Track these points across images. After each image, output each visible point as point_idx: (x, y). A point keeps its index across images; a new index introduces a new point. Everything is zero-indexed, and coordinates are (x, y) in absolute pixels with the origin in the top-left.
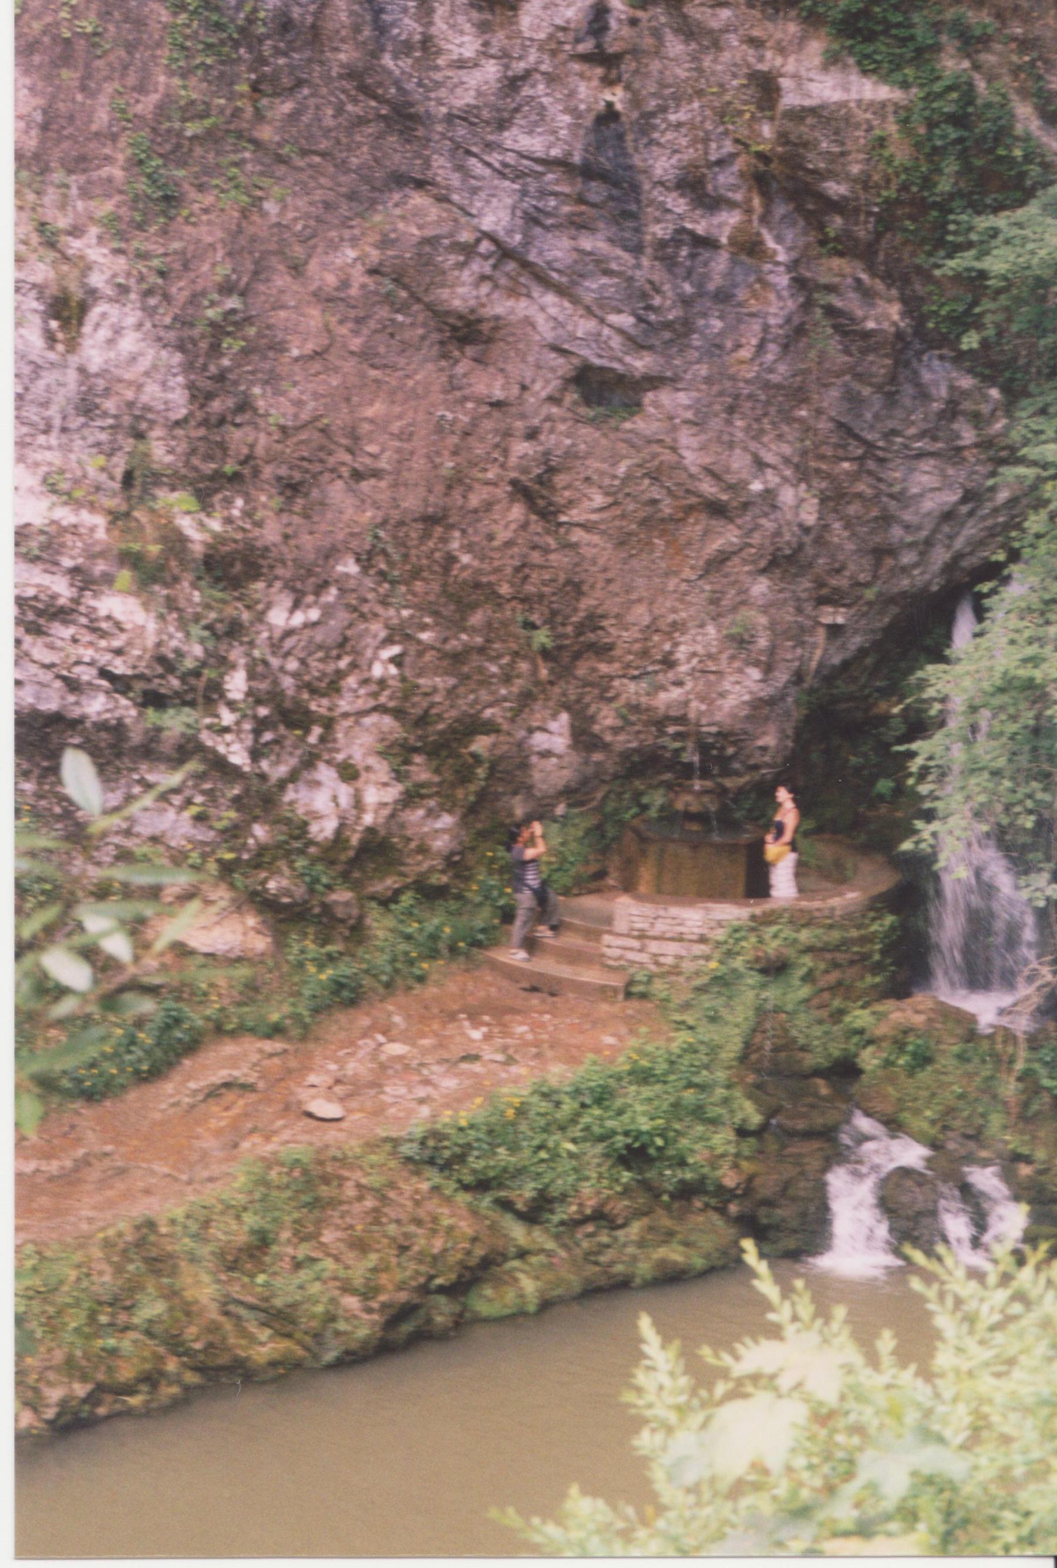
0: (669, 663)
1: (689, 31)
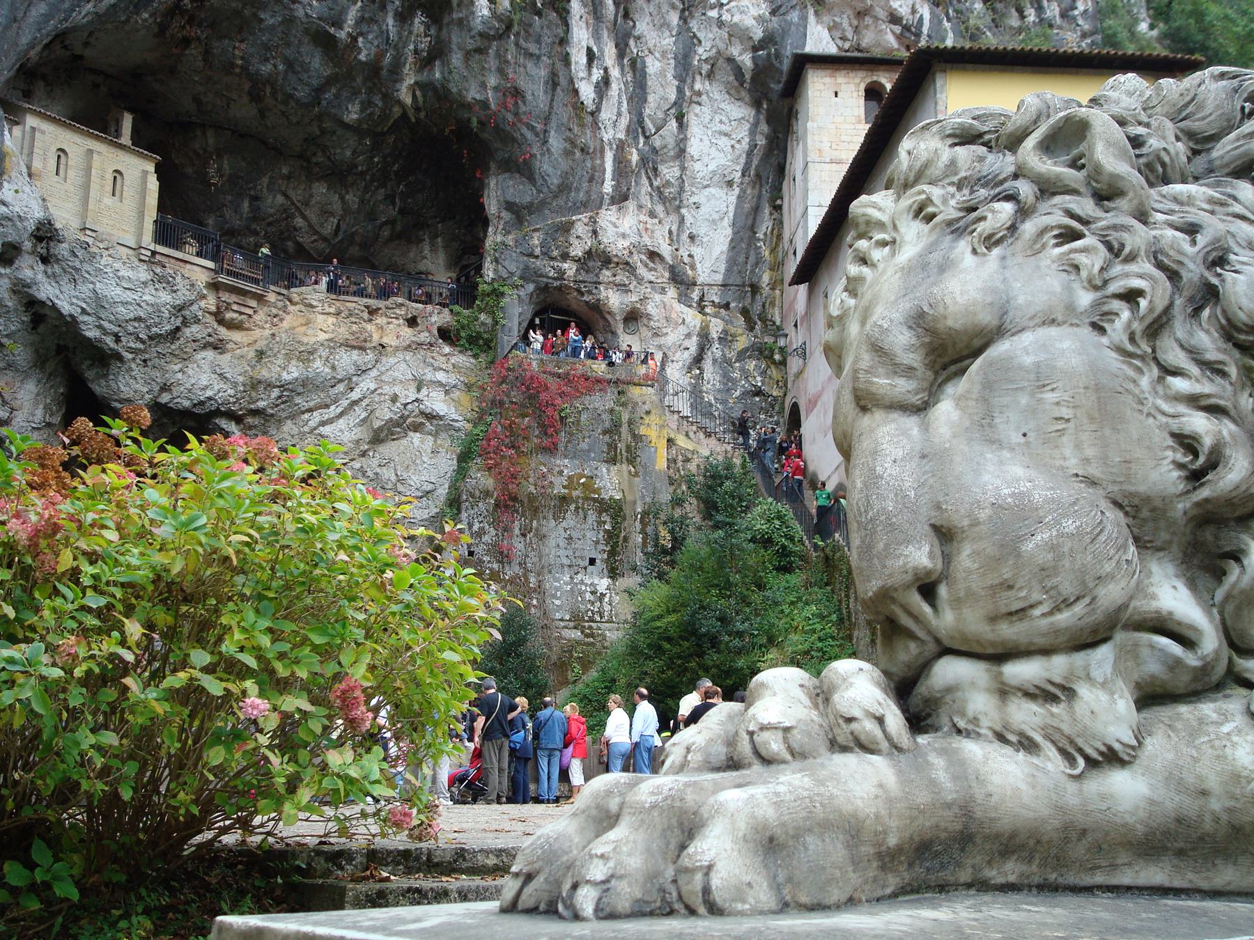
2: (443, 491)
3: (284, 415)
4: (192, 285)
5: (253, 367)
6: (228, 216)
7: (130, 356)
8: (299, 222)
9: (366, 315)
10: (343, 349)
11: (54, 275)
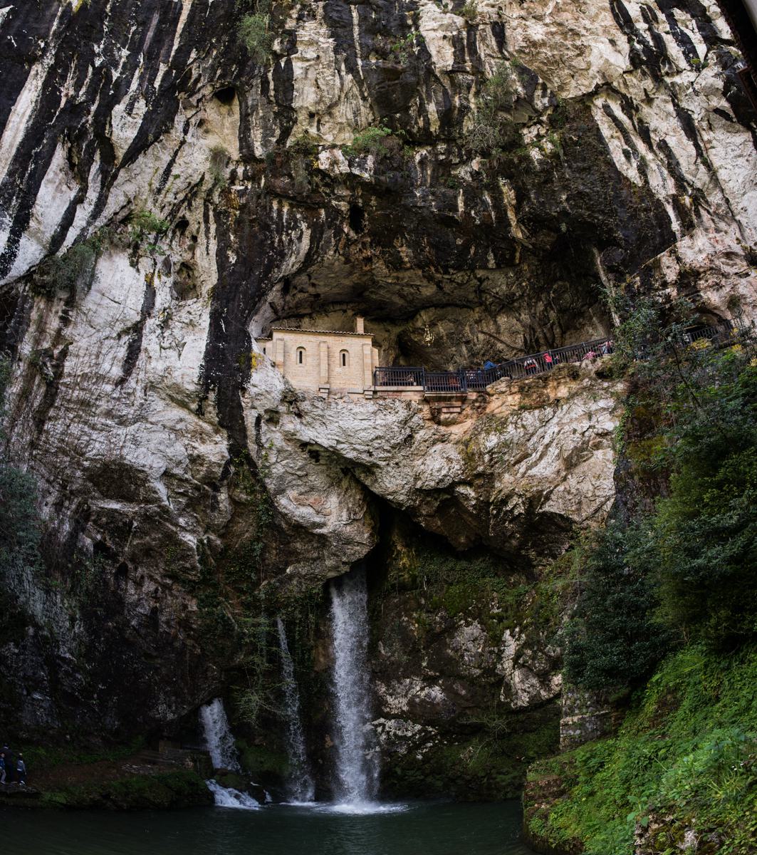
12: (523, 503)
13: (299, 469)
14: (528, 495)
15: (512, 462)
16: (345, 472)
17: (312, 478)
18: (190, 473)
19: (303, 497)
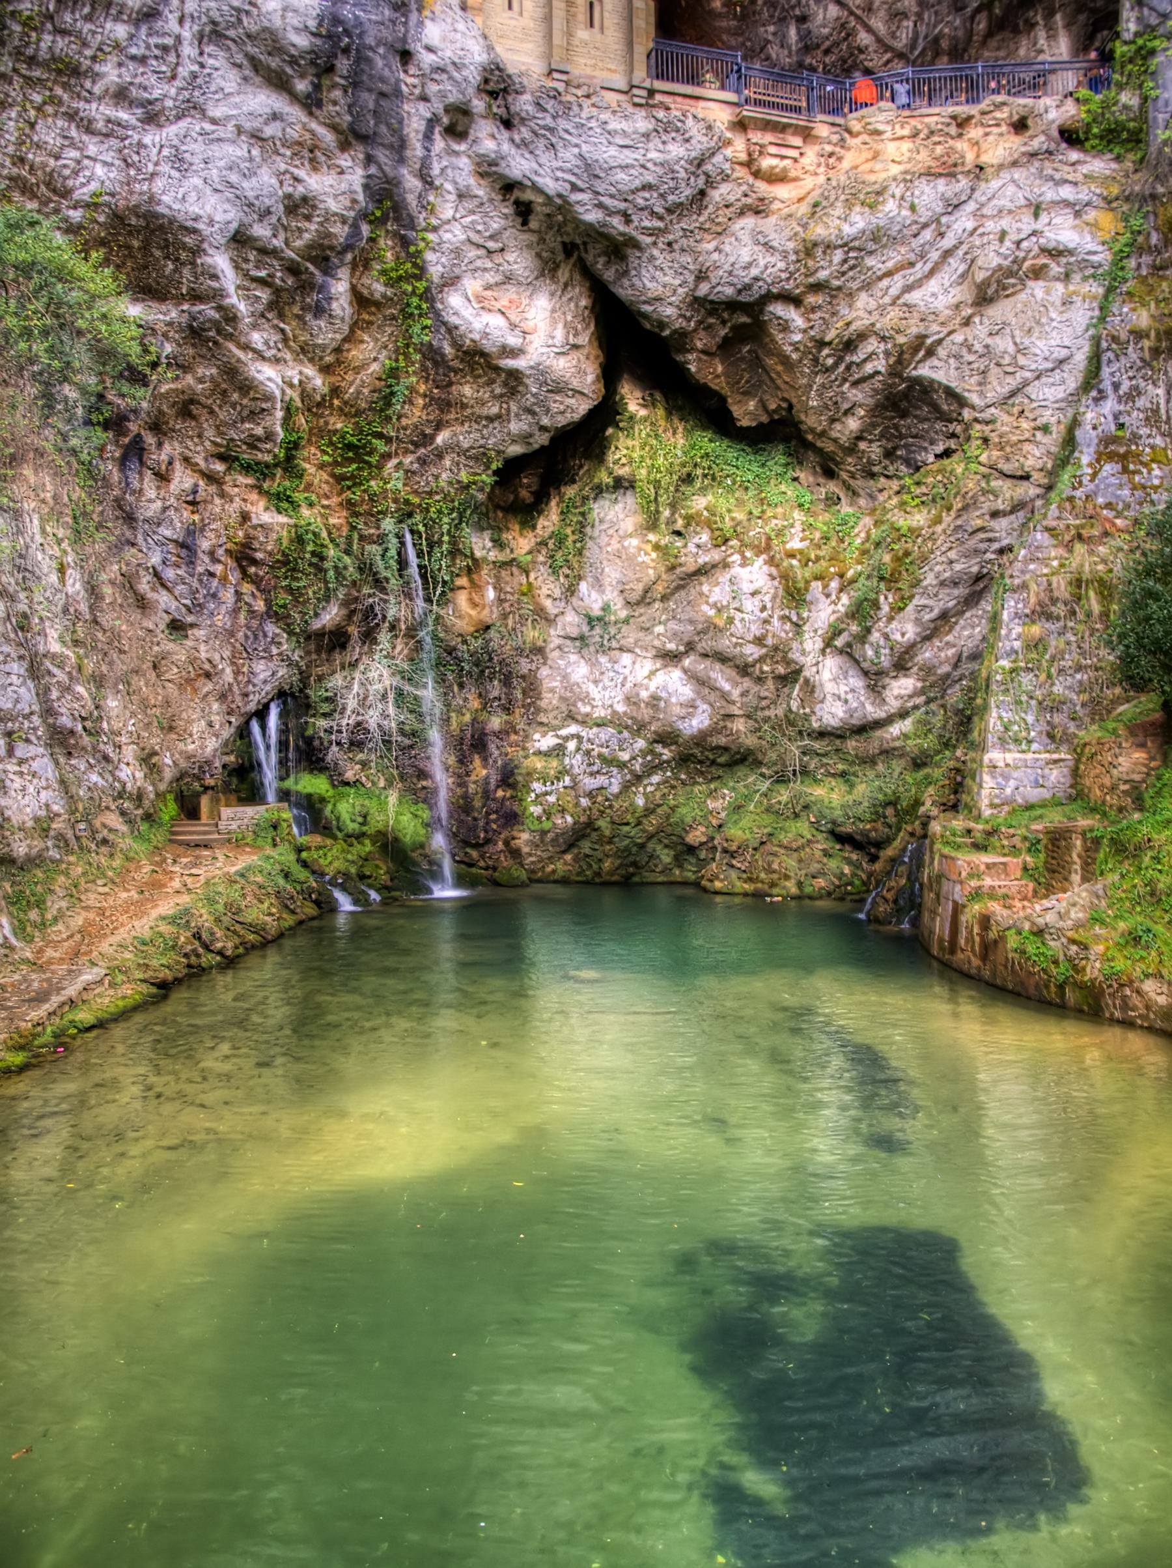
0: (191, 735)
1: (222, 495)
2: (1081, 358)
3: (854, 285)
4: (709, 128)
5: (805, 226)
6: (774, 56)
7: (649, 240)
8: (864, 38)
9: (953, 130)
10: (923, 180)
11: (524, 144)
12: (887, 354)
13: (491, 237)
14: (901, 340)
15: (879, 273)
16: (569, 249)
17: (511, 257)
18: (282, 236)
19: (489, 293)
